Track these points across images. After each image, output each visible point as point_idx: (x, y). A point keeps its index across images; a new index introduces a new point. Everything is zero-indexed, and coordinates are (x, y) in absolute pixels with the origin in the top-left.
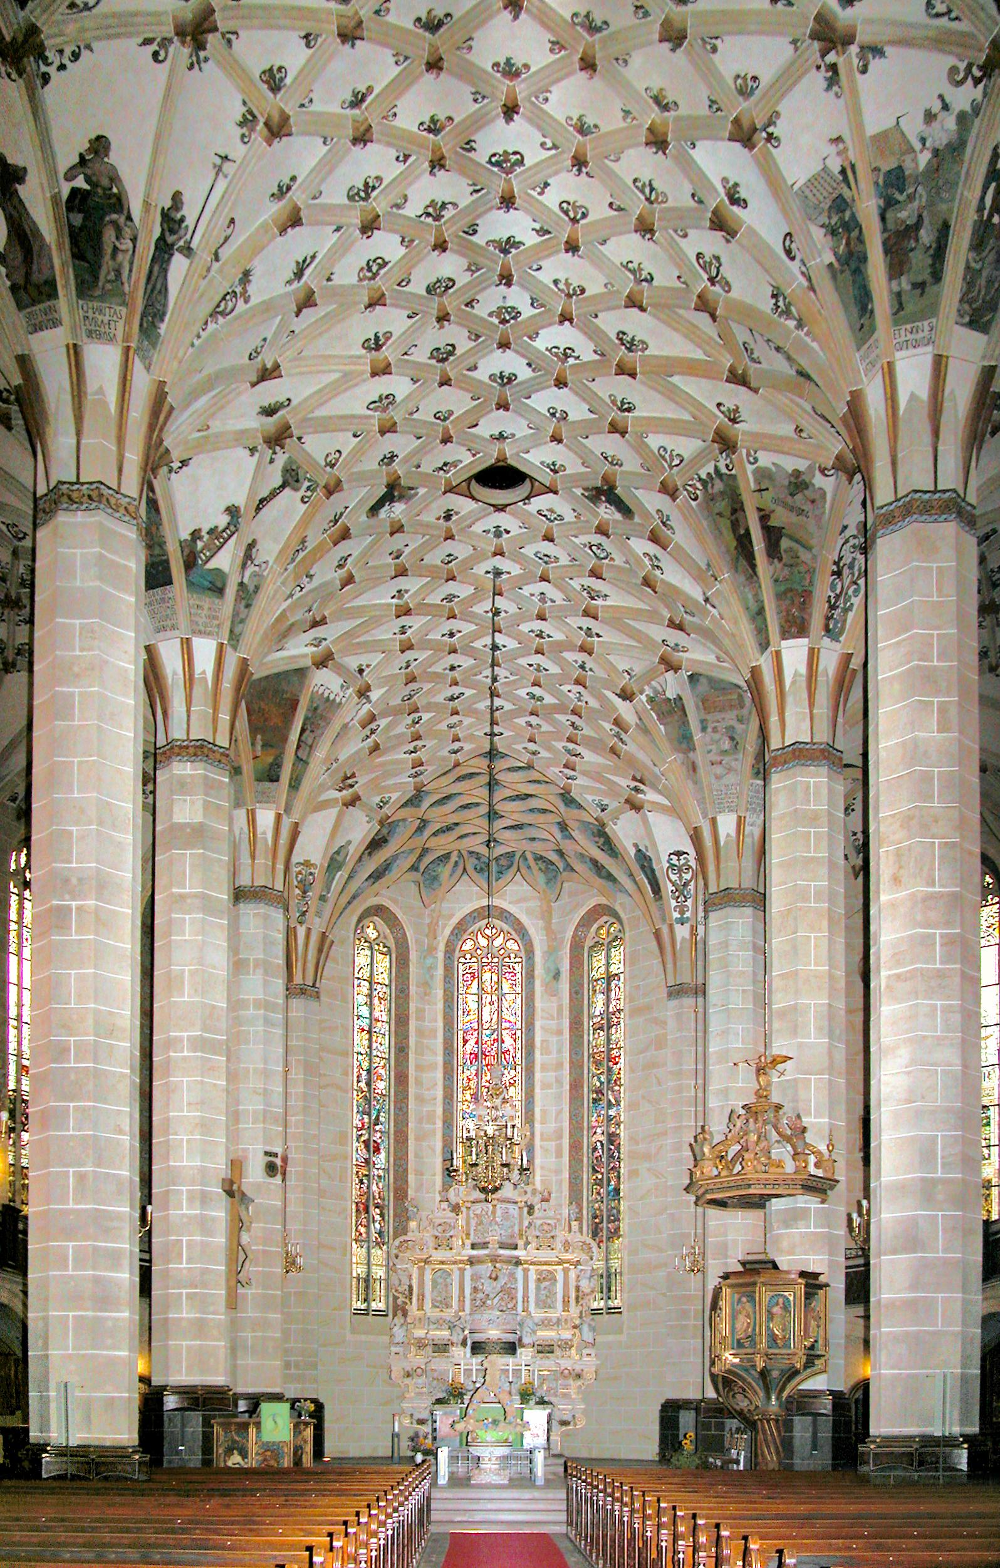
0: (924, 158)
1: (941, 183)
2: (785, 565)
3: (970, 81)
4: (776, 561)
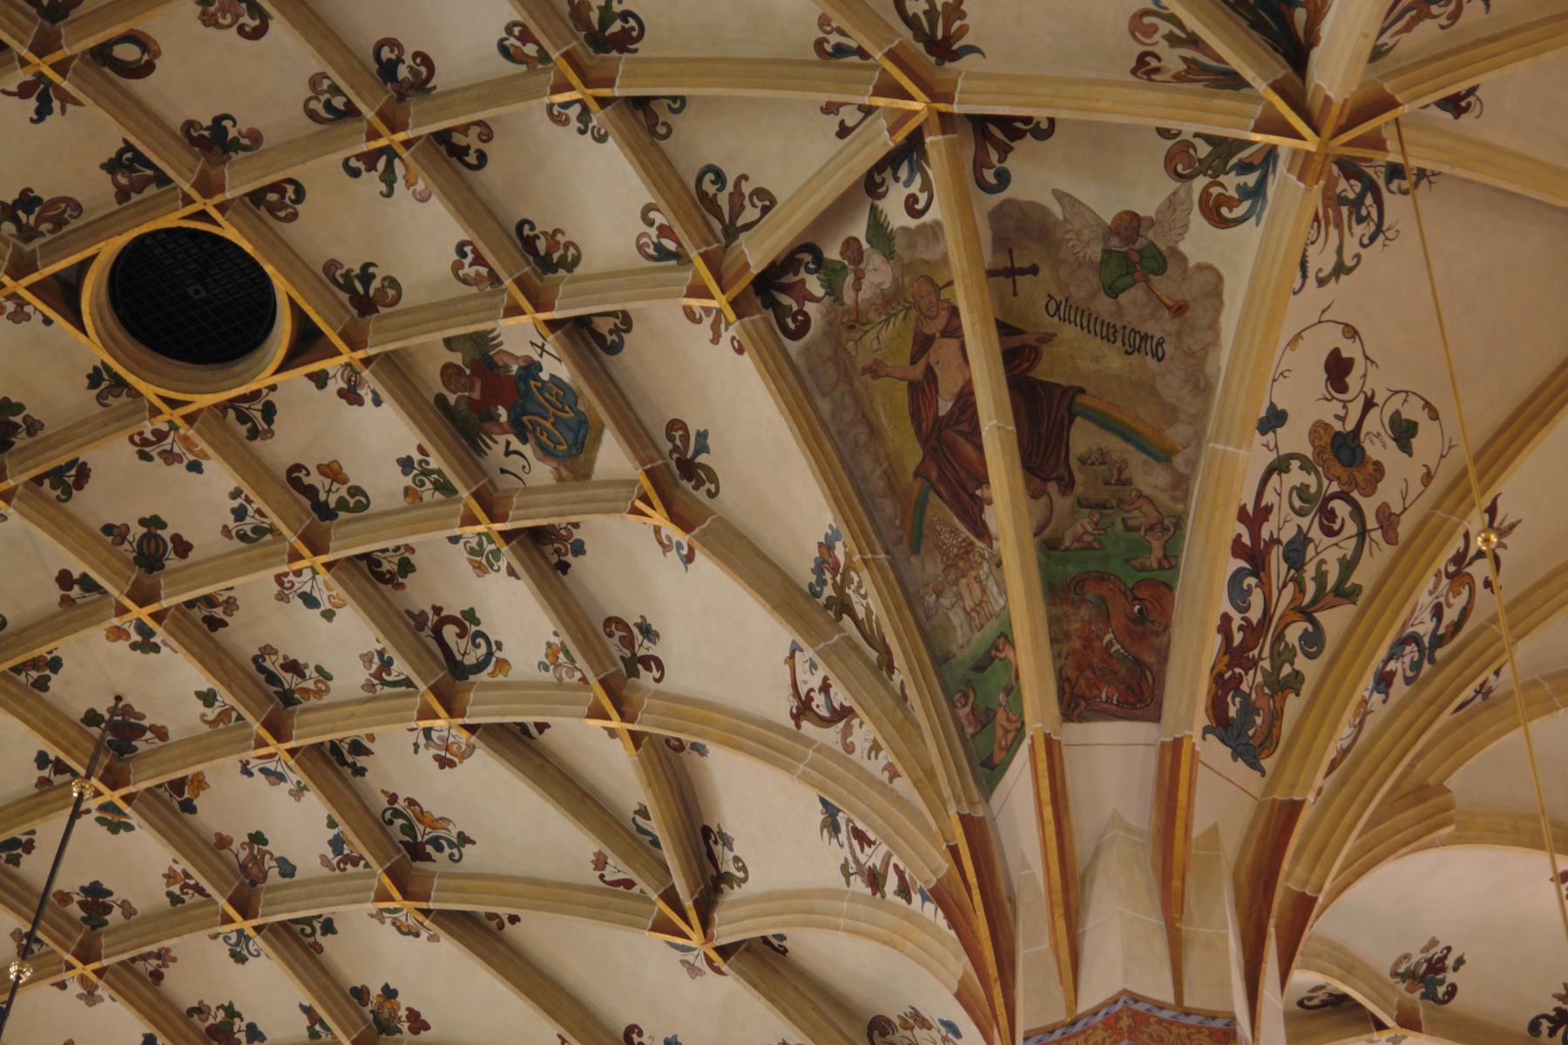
2: (1080, 503)
4: (1052, 487)
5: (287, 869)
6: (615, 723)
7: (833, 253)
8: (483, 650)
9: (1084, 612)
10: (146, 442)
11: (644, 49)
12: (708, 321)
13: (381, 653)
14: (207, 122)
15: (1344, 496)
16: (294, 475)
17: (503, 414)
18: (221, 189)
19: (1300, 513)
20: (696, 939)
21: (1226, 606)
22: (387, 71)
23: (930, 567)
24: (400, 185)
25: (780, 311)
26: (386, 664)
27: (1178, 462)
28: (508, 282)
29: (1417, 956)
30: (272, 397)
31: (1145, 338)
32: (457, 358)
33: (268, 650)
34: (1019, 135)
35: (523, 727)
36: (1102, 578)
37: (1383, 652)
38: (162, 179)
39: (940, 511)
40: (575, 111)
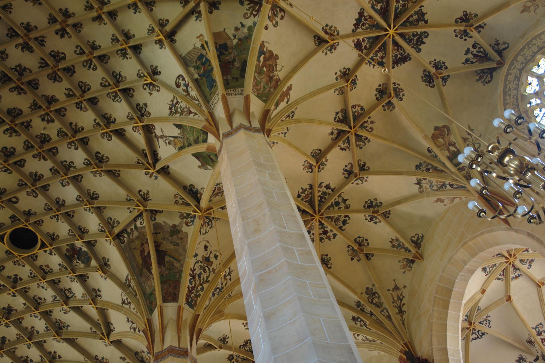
0: (235, 42)
1: (242, 48)
2: (166, 269)
3: (252, 16)
4: (162, 266)
5: (38, 332)
6: (93, 306)
7: (129, 230)
8: (72, 294)
9: (167, 286)
10: (15, 262)
11: (99, 199)
12: (109, 241)
13: (55, 296)
14: (27, 210)
15: (207, 267)
16: (41, 267)
17: (76, 256)
18: (29, 221)
19: (200, 269)
20: (107, 340)
21: (189, 284)
22: (58, 203)
23: (143, 279)
24: (59, 220)
25: (120, 240)
26: (56, 297)
27: (181, 262)
28: (77, 235)
29: (222, 337)
30: (37, 254)
31: (177, 243)
32: (68, 248)
33: (36, 296)
34: (157, 212)
35: (79, 307)
36: (170, 280)
37: (213, 290)
38: (19, 220)
39: (145, 271)
40: (88, 209)
